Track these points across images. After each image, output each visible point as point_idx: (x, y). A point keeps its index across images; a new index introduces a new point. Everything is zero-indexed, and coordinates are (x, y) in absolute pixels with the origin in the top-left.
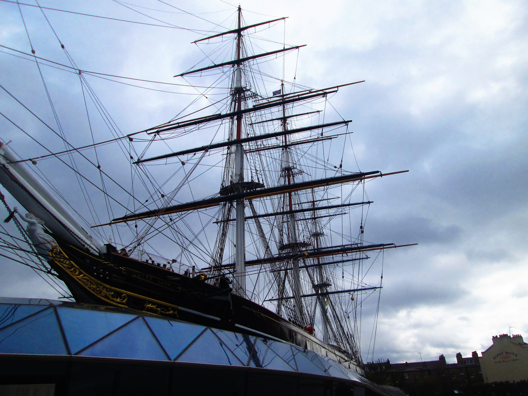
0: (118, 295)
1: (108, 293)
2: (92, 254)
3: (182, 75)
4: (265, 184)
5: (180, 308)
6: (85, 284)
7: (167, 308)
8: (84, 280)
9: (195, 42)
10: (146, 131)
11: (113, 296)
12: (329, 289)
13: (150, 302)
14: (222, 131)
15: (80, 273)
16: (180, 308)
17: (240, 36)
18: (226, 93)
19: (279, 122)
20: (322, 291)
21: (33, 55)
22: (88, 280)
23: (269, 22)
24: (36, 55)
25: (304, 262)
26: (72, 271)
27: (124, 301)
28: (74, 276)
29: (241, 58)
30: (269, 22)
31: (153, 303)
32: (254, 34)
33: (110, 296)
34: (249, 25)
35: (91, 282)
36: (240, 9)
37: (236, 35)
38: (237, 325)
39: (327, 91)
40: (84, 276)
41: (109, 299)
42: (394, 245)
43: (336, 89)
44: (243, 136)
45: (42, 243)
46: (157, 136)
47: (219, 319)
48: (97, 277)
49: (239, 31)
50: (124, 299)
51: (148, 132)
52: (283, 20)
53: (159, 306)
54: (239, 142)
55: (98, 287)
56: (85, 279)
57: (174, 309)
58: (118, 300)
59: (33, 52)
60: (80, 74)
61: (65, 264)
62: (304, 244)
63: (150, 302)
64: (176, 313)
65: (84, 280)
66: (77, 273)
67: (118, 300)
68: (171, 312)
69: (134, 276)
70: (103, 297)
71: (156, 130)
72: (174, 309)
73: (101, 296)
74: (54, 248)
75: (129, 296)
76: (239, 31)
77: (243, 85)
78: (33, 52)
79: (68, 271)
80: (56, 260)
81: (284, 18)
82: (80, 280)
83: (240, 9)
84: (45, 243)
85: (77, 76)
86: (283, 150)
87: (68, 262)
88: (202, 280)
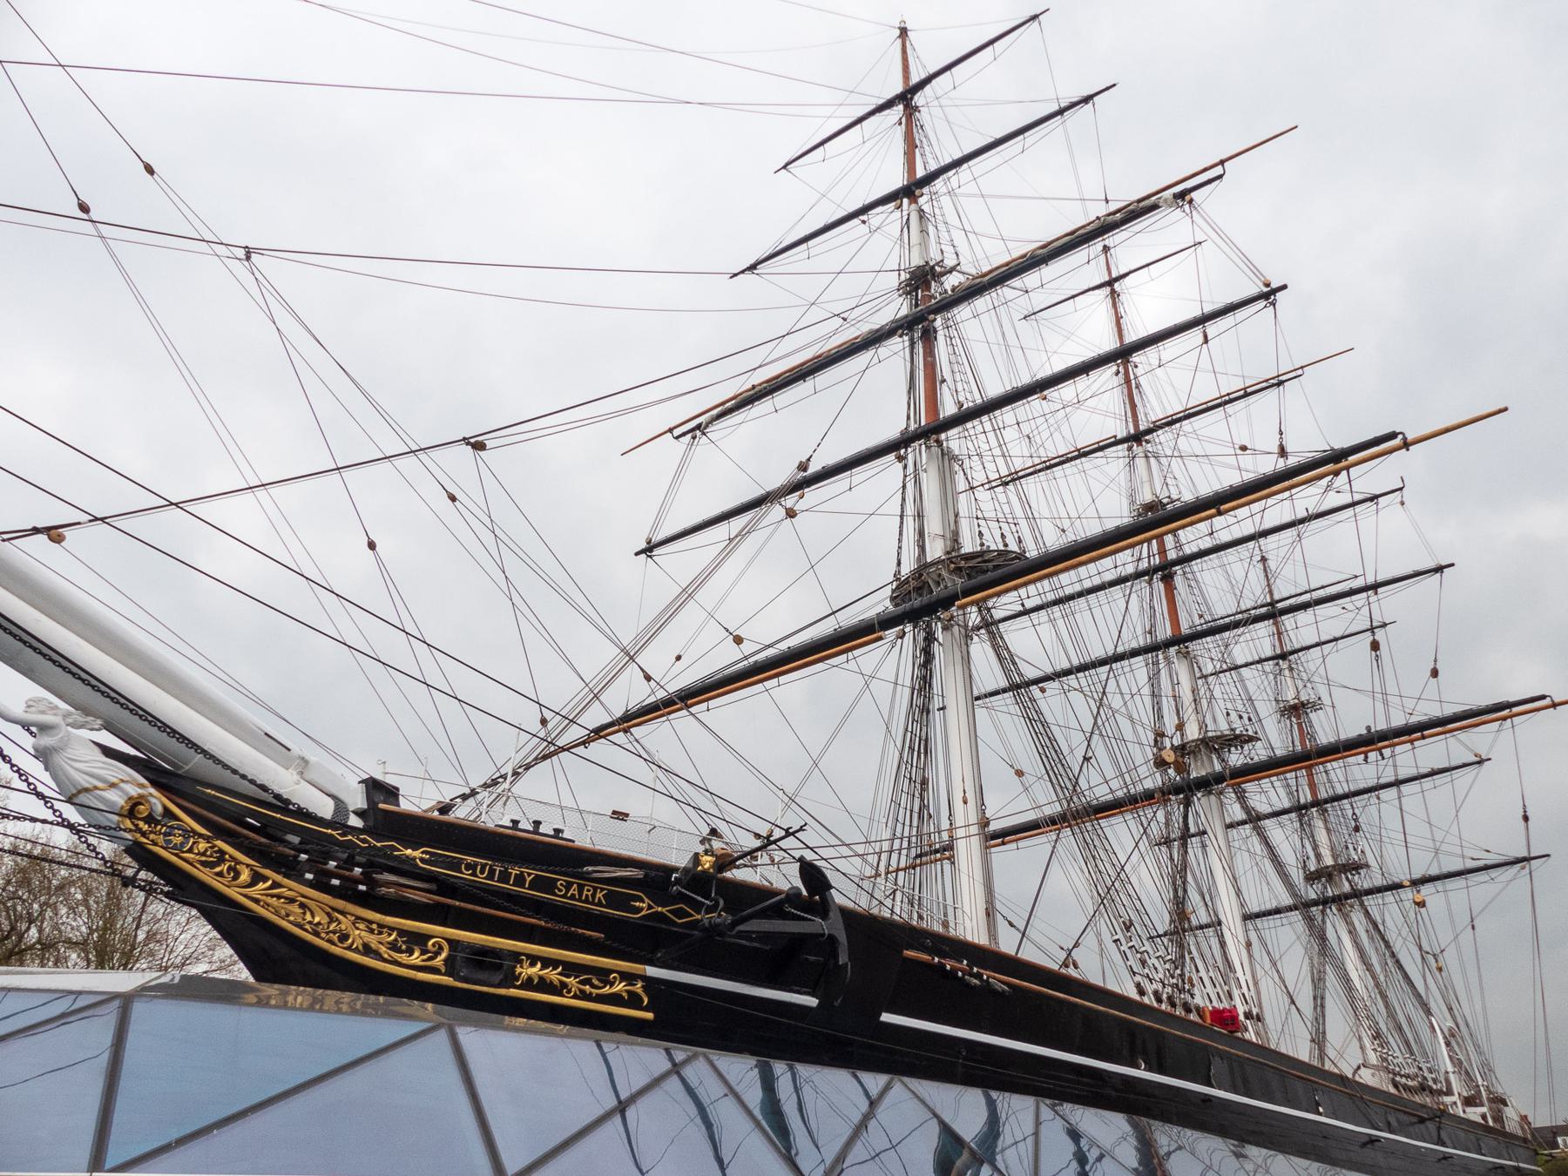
0: (417, 940)
1: (373, 940)
3: (753, 267)
5: (651, 971)
6: (277, 913)
7: (604, 974)
8: (269, 900)
9: (784, 167)
11: (393, 947)
12: (1363, 881)
13: (534, 959)
15: (257, 878)
16: (651, 971)
21: (84, 216)
22: (291, 901)
24: (94, 215)
25: (1242, 798)
26: (220, 874)
27: (438, 962)
28: (233, 893)
31: (547, 962)
32: (953, 94)
33: (383, 949)
35: (302, 906)
36: (904, 32)
38: (886, 1017)
40: (276, 885)
41: (377, 955)
42: (1547, 702)
44: (948, 409)
45: (86, 790)
47: (812, 1002)
48: (321, 885)
50: (437, 954)
52: (1035, 24)
53: (570, 968)
54: (932, 431)
55: (332, 920)
56: (279, 897)
57: (628, 977)
59: (84, 208)
60: (248, 258)
61: (190, 851)
63: (534, 959)
64: (638, 987)
65: (269, 900)
66: (245, 876)
67: (416, 958)
68: (620, 987)
69: (466, 875)
70: (356, 950)
72: (628, 977)
73: (349, 948)
74: (134, 804)
76: (906, 98)
78: (84, 208)
79: (205, 876)
80: (155, 844)
81: (1034, 17)
82: (257, 901)
83: (904, 32)
84: (96, 788)
85: (240, 268)
87: (202, 846)
88: (704, 872)
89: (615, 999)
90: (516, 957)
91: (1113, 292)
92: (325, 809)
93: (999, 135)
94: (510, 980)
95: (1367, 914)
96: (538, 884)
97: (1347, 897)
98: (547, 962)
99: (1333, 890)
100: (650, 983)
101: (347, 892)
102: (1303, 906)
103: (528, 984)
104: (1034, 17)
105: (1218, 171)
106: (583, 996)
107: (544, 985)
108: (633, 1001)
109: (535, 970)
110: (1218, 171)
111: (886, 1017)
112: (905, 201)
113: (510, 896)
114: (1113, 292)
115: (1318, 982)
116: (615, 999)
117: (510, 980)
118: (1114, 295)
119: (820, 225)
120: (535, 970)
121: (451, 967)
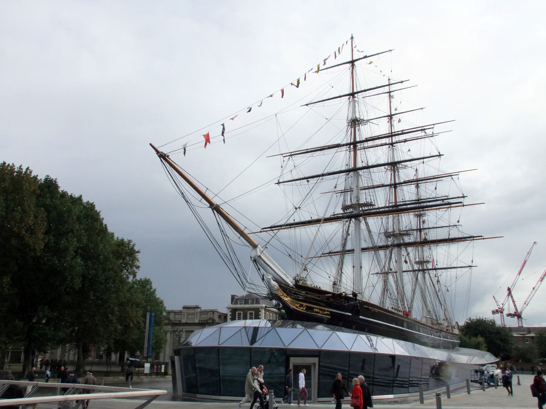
0: (301, 306)
3: (307, 105)
5: (331, 310)
7: (324, 310)
14: (341, 159)
16: (331, 310)
17: (353, 66)
18: (344, 124)
29: (355, 91)
31: (318, 309)
37: (349, 65)
38: (361, 317)
39: (425, 128)
43: (433, 126)
46: (291, 158)
47: (350, 314)
48: (293, 298)
49: (352, 62)
53: (321, 310)
62: (407, 233)
67: (302, 308)
68: (326, 313)
71: (289, 154)
72: (328, 311)
75: (306, 306)
76: (352, 62)
77: (358, 116)
86: (389, 147)
89: (325, 314)
90: (314, 308)
91: (390, 95)
93: (378, 86)
95: (429, 274)
99: (423, 267)
100: (331, 312)
105: (433, 126)
106: (322, 314)
107: (317, 312)
108: (328, 315)
111: (361, 317)
112: (351, 97)
114: (390, 95)
116: (325, 314)
117: (313, 311)
120: (316, 310)
121: (306, 310)
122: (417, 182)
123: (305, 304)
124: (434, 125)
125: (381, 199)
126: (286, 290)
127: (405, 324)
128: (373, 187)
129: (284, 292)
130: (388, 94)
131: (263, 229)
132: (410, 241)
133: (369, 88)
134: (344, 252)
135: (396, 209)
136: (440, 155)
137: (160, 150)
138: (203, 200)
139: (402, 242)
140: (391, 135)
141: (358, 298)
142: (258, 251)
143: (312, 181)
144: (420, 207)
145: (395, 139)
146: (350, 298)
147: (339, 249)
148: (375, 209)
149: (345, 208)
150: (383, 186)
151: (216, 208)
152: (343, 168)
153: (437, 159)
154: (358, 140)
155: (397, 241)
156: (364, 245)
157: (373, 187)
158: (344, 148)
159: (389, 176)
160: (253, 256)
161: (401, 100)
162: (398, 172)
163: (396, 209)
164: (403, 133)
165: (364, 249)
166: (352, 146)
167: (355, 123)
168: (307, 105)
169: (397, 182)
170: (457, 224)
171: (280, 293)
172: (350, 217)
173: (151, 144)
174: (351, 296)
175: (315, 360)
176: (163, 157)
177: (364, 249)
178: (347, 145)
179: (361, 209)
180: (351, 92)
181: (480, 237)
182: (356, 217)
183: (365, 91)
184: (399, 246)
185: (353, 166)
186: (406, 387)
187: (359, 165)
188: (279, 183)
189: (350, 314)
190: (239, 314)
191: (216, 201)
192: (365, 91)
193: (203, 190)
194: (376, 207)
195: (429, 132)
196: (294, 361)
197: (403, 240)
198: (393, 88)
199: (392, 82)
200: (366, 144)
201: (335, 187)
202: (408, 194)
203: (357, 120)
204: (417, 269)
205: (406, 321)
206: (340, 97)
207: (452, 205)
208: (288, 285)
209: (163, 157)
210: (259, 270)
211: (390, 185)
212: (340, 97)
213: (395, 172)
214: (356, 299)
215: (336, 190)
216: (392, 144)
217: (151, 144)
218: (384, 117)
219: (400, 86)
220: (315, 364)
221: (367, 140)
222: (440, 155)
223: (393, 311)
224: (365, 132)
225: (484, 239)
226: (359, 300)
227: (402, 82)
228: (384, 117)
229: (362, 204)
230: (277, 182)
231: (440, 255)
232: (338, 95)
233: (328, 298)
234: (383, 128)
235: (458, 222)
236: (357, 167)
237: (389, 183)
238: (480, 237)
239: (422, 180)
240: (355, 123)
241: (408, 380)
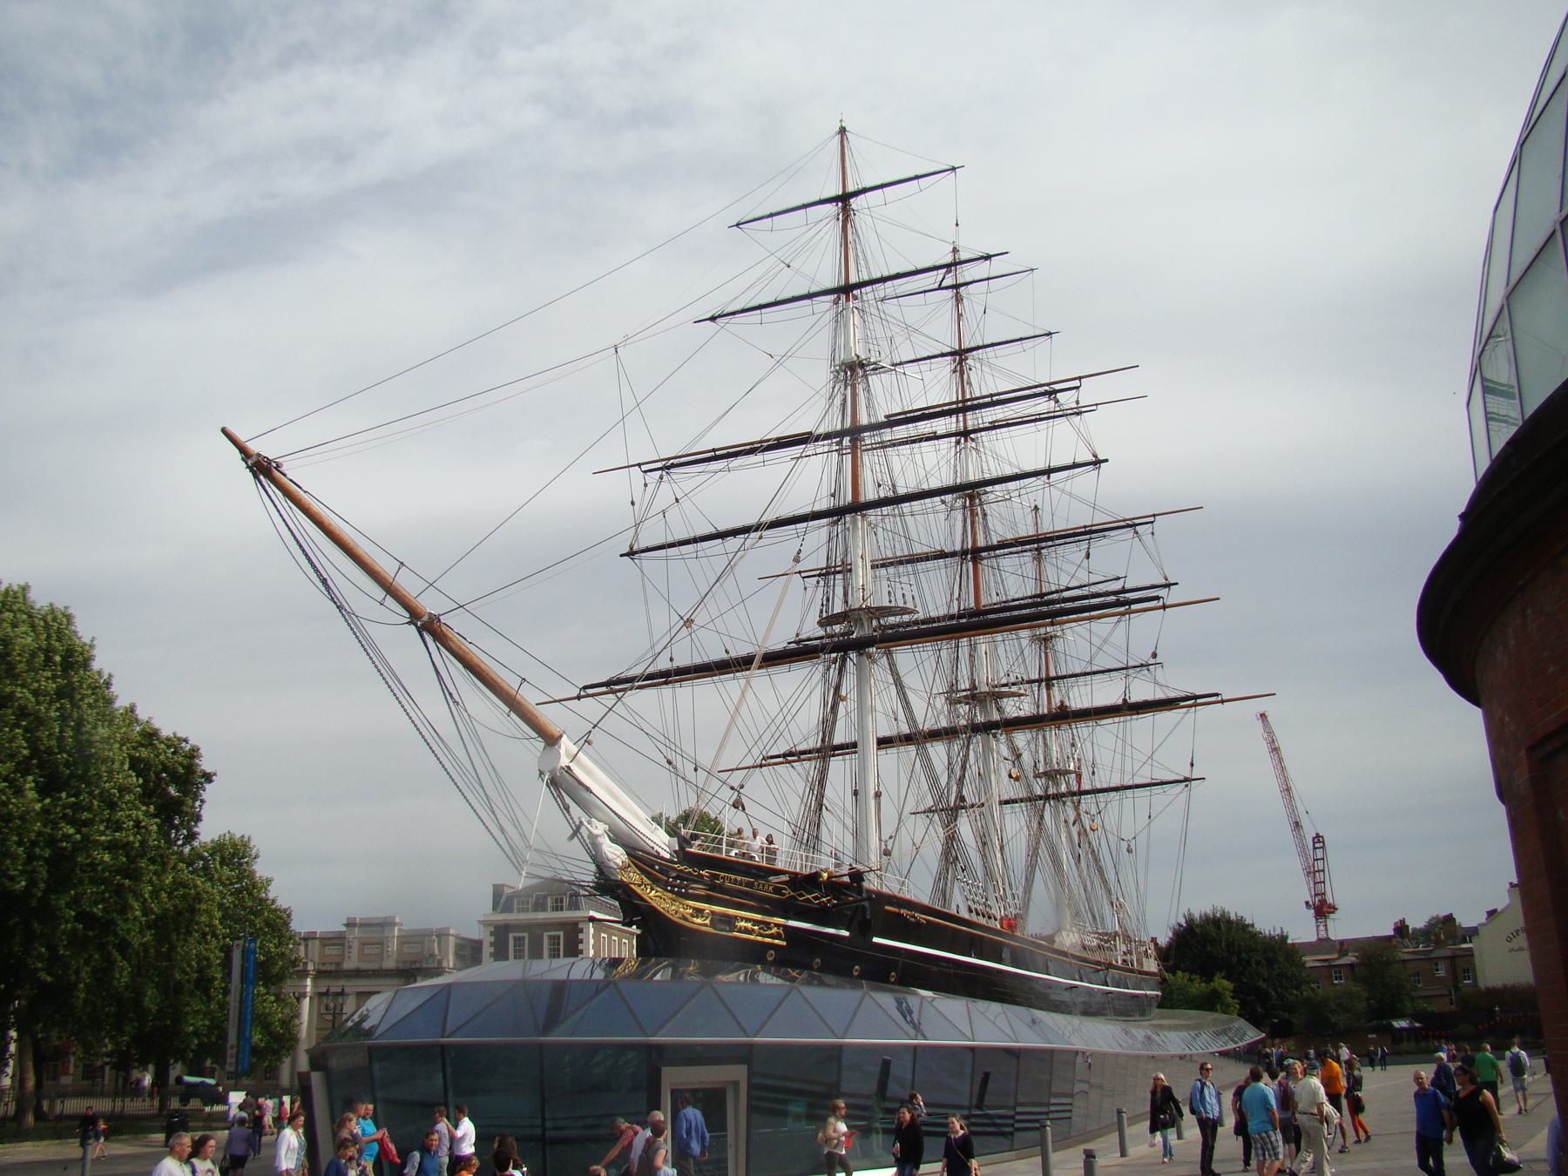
0: (699, 912)
2: (663, 858)
3: (713, 319)
4: (919, 609)
7: (768, 925)
10: (639, 465)
17: (846, 210)
18: (822, 375)
19: (947, 364)
20: (1055, 791)
23: (917, 177)
29: (853, 279)
30: (917, 177)
31: (748, 920)
34: (868, 185)
36: (843, 131)
38: (875, 940)
39: (1057, 387)
47: (846, 933)
48: (672, 891)
51: (644, 468)
53: (756, 922)
58: (699, 921)
63: (743, 919)
67: (699, 921)
68: (775, 930)
71: (659, 465)
72: (777, 925)
75: (713, 913)
76: (844, 199)
86: (958, 443)
92: (668, 856)
93: (921, 266)
94: (733, 928)
96: (749, 885)
97: (1063, 795)
98: (748, 920)
100: (786, 928)
101: (679, 894)
102: (1031, 799)
103: (740, 931)
104: (954, 169)
105: (1076, 383)
107: (746, 931)
108: (778, 936)
109: (743, 924)
110: (1076, 383)
111: (875, 940)
112: (843, 297)
113: (741, 891)
115: (1033, 853)
117: (733, 928)
118: (959, 299)
119: (772, 299)
120: (743, 924)
121: (712, 924)
122: (1038, 543)
123: (707, 907)
124: (1080, 378)
125: (934, 594)
126: (652, 867)
127: (1006, 954)
128: (913, 559)
129: (643, 871)
130: (950, 293)
131: (585, 688)
132: (1022, 714)
133: (893, 272)
134: (827, 751)
135: (977, 622)
136: (1097, 463)
137: (254, 447)
138: (390, 601)
139: (996, 716)
140: (963, 407)
141: (866, 884)
142: (562, 751)
143: (733, 543)
144: (1043, 612)
145: (973, 419)
146: (844, 884)
147: (813, 742)
148: (916, 623)
149: (825, 622)
150: (942, 555)
151: (430, 627)
152: (823, 505)
153: (1088, 475)
154: (864, 420)
155: (980, 718)
156: (885, 732)
157: (913, 559)
158: (822, 446)
159: (959, 525)
160: (546, 769)
161: (991, 313)
162: (985, 515)
163: (977, 622)
164: (994, 401)
165: (884, 742)
166: (846, 441)
167: (853, 371)
168: (713, 319)
169: (981, 543)
170: (1152, 661)
171: (633, 877)
172: (843, 647)
173: (224, 431)
174: (846, 879)
175: (739, 1072)
176: (262, 469)
177: (884, 742)
178: (827, 436)
179: (875, 623)
180: (843, 283)
181: (1213, 698)
182: (861, 645)
183: (883, 280)
184: (988, 728)
185: (849, 498)
186: (1004, 1134)
187: (869, 493)
188: (631, 554)
189: (846, 933)
190: (519, 941)
191: (430, 604)
192: (883, 280)
193: (387, 567)
194: (921, 616)
195: (1066, 399)
196: (674, 1077)
197: (999, 709)
198: (967, 273)
199: (963, 256)
200: (887, 435)
201: (797, 560)
202: (1012, 580)
203: (862, 366)
204: (1039, 792)
205: (1008, 946)
206: (810, 296)
207: (1134, 607)
208: (658, 856)
209: (262, 469)
210: (567, 809)
211: (964, 553)
212: (810, 296)
213: (973, 514)
214: (860, 889)
215: (800, 567)
216: (965, 434)
217: (224, 431)
218: (943, 355)
219: (980, 270)
220: (736, 1084)
221: (892, 422)
222: (1097, 463)
223: (974, 918)
224: (885, 396)
225: (1223, 701)
226: (869, 892)
227: (988, 257)
228: (943, 355)
229: (878, 609)
230: (627, 550)
231: (1104, 751)
232: (804, 291)
233: (777, 890)
234: (936, 386)
235: (1154, 655)
236: (862, 499)
237: (958, 547)
238: (1213, 698)
239: (1051, 539)
240: (853, 371)
241: (1011, 1113)
